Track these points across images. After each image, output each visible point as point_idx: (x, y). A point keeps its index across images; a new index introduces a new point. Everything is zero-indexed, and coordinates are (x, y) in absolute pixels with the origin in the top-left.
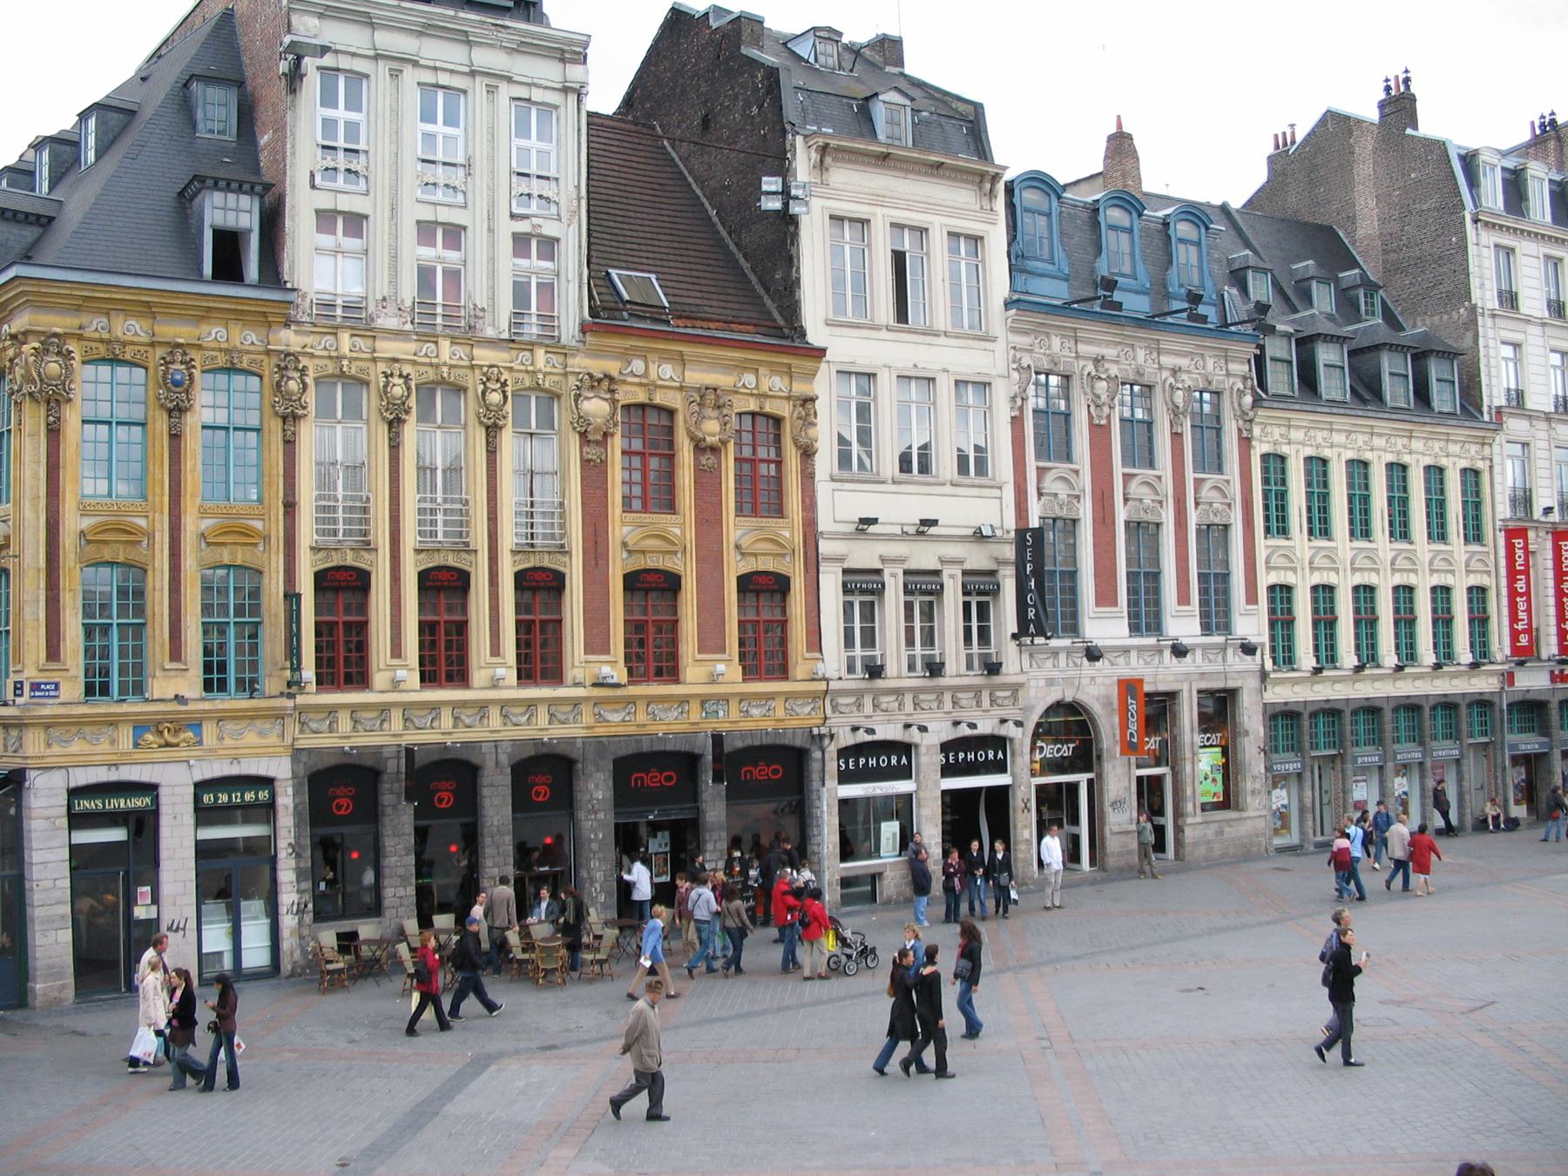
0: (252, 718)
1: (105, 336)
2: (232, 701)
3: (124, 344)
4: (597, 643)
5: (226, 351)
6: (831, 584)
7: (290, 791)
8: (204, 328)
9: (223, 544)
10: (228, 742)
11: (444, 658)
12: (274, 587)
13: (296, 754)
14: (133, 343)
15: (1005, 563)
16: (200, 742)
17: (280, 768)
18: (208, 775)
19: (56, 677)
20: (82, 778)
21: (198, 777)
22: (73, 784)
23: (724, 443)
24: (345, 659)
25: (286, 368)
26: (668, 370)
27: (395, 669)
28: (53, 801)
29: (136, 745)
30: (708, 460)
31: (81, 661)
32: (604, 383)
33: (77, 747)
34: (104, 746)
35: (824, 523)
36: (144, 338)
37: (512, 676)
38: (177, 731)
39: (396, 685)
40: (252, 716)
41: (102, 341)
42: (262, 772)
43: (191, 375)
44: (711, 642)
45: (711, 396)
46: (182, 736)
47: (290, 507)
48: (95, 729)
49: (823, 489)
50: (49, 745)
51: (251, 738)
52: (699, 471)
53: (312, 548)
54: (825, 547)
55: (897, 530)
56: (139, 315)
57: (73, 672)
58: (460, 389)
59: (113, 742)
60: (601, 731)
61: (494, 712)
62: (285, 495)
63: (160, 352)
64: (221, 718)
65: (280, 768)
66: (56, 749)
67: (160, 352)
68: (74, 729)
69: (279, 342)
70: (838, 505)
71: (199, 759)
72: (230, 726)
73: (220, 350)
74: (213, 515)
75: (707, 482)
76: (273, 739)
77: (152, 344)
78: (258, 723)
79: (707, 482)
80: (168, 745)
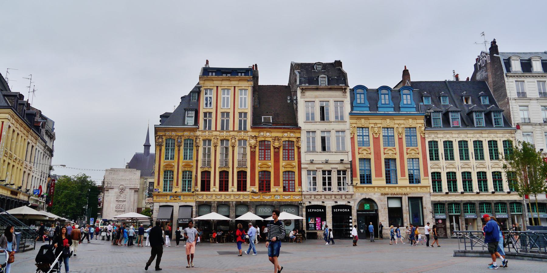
2: (187, 192)
4: (253, 184)
6: (304, 173)
11: (224, 187)
12: (194, 174)
13: (196, 202)
15: (348, 168)
17: (193, 204)
20: (162, 204)
23: (280, 147)
24: (205, 186)
26: (268, 134)
27: (215, 188)
30: (276, 150)
31: (163, 186)
32: (256, 137)
33: (161, 199)
35: (303, 161)
37: (218, 190)
39: (214, 191)
40: (189, 195)
44: (277, 184)
45: (277, 138)
47: (197, 161)
49: (303, 155)
51: (189, 199)
52: (275, 152)
54: (303, 166)
55: (321, 162)
58: (228, 140)
60: (253, 200)
61: (214, 196)
64: (184, 195)
65: (193, 204)
70: (305, 158)
75: (277, 155)
79: (277, 155)
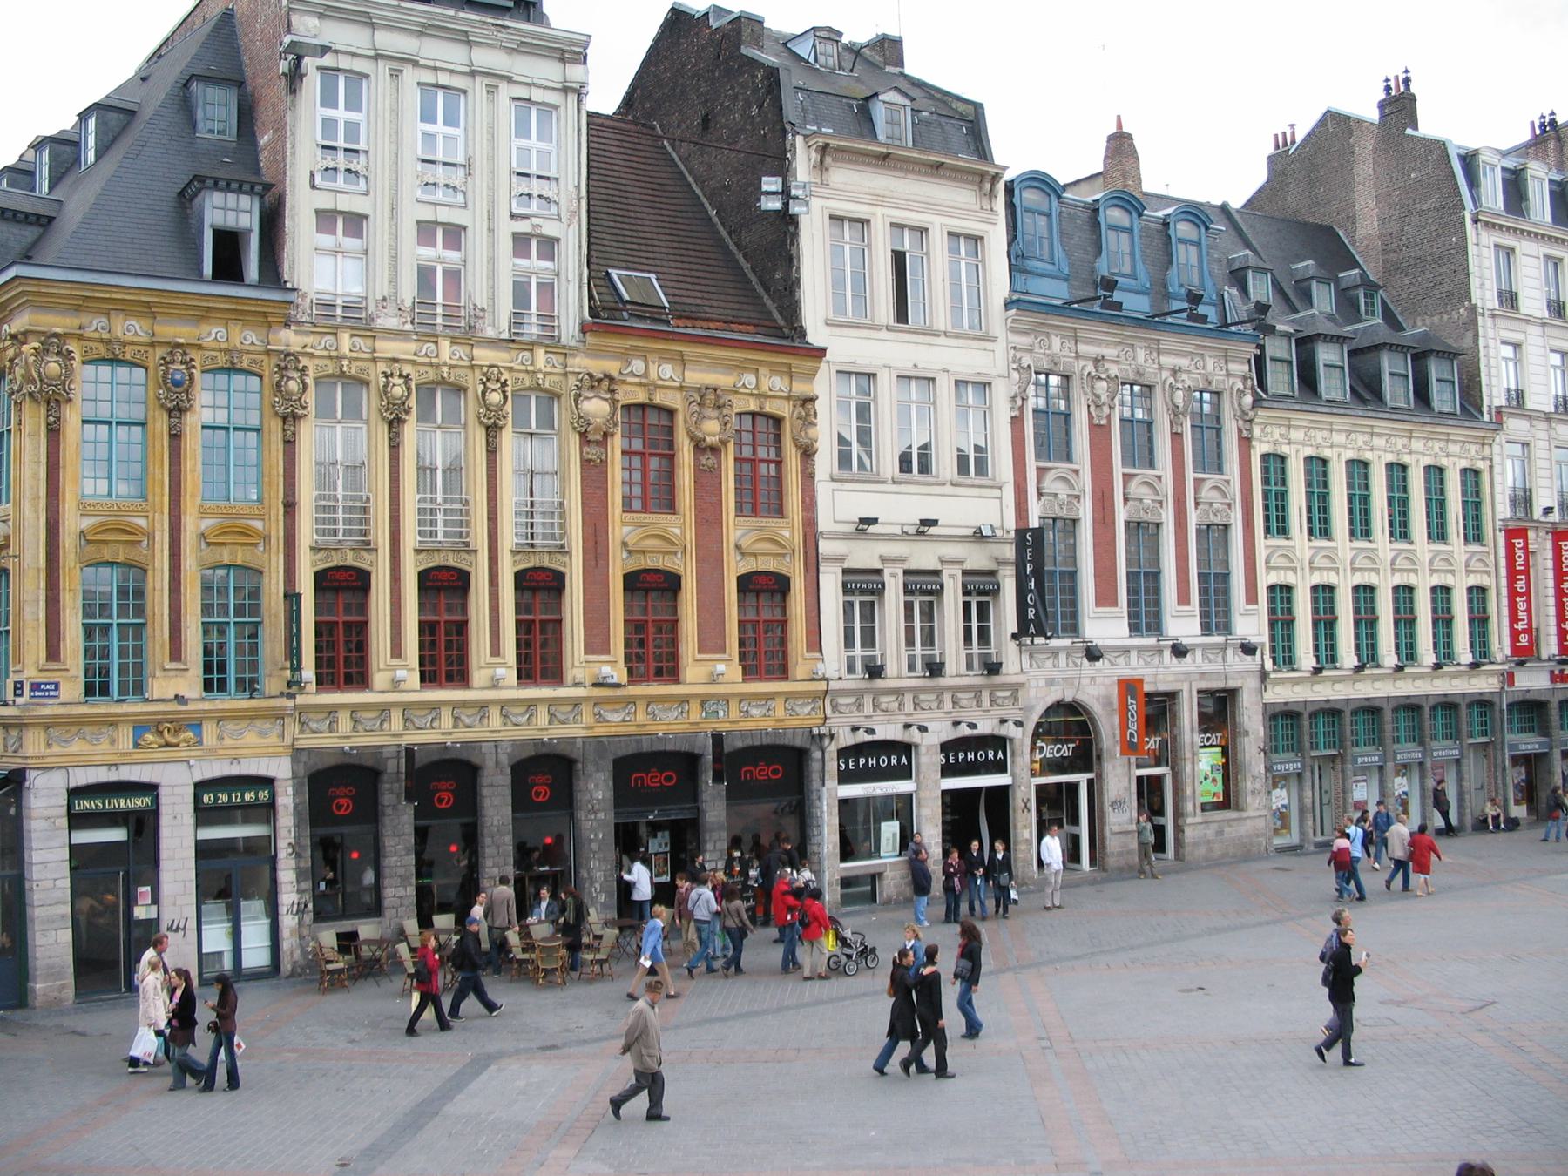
0: (252, 718)
1: (105, 336)
3: (124, 344)
5: (226, 351)
7: (290, 791)
8: (204, 328)
9: (223, 544)
10: (228, 742)
12: (274, 587)
13: (296, 754)
14: (133, 343)
16: (200, 742)
17: (280, 768)
18: (208, 775)
19: (56, 677)
20: (82, 778)
21: (198, 777)
22: (73, 784)
24: (345, 659)
25: (286, 368)
28: (53, 801)
29: (136, 745)
33: (77, 747)
34: (104, 746)
36: (144, 338)
38: (177, 731)
40: (252, 716)
41: (102, 341)
42: (262, 772)
43: (191, 375)
46: (182, 736)
47: (290, 507)
48: (95, 729)
50: (49, 745)
51: (251, 738)
53: (312, 548)
56: (139, 315)
57: (73, 672)
59: (113, 742)
62: (285, 495)
63: (160, 352)
64: (221, 718)
65: (280, 768)
66: (56, 749)
67: (160, 352)
68: (74, 729)
69: (279, 342)
71: (199, 759)
72: (230, 726)
73: (220, 350)
74: (213, 515)
76: (273, 739)
77: (152, 344)
78: (258, 723)
80: (168, 745)
